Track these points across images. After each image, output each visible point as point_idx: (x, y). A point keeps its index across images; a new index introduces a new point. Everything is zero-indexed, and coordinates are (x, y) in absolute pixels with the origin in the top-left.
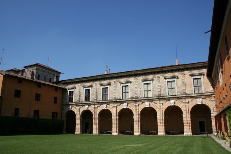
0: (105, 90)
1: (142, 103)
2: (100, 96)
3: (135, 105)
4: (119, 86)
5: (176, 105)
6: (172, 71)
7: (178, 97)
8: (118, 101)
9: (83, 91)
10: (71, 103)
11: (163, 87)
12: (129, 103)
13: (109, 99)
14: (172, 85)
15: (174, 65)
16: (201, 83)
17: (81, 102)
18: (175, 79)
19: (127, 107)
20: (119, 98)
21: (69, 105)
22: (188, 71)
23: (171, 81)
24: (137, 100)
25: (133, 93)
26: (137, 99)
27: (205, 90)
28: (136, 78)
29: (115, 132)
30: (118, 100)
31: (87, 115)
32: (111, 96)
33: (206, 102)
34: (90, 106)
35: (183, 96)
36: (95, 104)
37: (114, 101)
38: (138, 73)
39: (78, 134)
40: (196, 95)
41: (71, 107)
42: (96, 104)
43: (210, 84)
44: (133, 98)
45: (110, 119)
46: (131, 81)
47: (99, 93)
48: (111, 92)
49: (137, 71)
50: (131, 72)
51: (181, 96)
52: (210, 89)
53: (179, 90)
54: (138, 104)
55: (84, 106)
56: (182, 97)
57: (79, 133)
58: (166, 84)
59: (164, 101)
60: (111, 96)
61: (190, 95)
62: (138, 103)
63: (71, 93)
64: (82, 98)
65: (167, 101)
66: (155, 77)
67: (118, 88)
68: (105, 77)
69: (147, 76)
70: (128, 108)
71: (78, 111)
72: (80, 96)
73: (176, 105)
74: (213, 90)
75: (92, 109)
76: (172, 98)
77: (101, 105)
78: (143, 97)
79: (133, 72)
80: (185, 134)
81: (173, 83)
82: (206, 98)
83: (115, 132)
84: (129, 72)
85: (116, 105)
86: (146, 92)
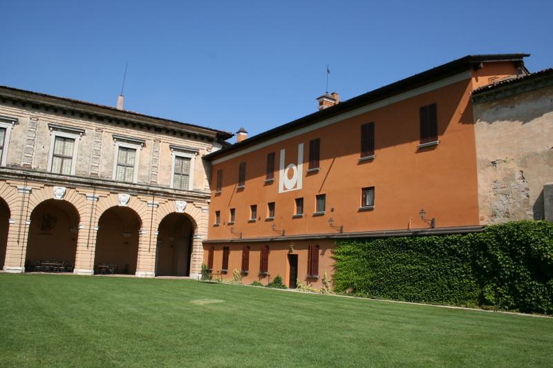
3: (22, 187)
5: (130, 206)
6: (134, 125)
7: (138, 189)
14: (126, 158)
15: (113, 107)
16: (188, 168)
18: (138, 147)
22: (169, 135)
23: (65, 139)
24: (29, 176)
25: (19, 153)
26: (31, 174)
27: (195, 185)
28: (36, 114)
33: (191, 210)
35: (151, 188)
38: (46, 102)
40: (177, 192)
43: (205, 176)
44: (15, 166)
45: (161, 242)
46: (17, 119)
49: (46, 98)
51: (145, 188)
53: (143, 174)
58: (114, 152)
59: (105, 193)
61: (165, 190)
62: (30, 186)
66: (91, 127)
74: (208, 188)
76: (124, 188)
78: (49, 171)
79: (31, 96)
80: (140, 274)
81: (130, 154)
82: (77, 189)
84: (20, 93)
86: (58, 161)
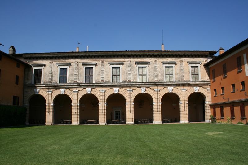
0: (89, 71)
1: (109, 88)
2: (82, 78)
3: (129, 90)
4: (108, 68)
5: (174, 92)
6: (170, 56)
7: (176, 84)
8: (106, 85)
9: (58, 70)
10: (39, 85)
11: (160, 73)
12: (121, 88)
13: (94, 82)
14: (169, 71)
15: (160, 50)
16: (198, 71)
17: (55, 84)
18: (173, 66)
19: (118, 92)
20: (107, 81)
21: (36, 87)
22: (186, 58)
23: (142, 67)
24: (131, 85)
25: (126, 76)
26: (131, 84)
27: (202, 78)
28: (130, 59)
29: (103, 122)
30: (108, 84)
31: (63, 103)
32: (96, 78)
33: (202, 91)
34: (67, 90)
35: (182, 83)
36: (75, 88)
37: (101, 84)
38: (133, 54)
39: (50, 125)
40: (194, 83)
41: (38, 90)
42: (76, 88)
43: (206, 74)
44: (125, 82)
45: (190, 106)
47: (80, 74)
48: (97, 73)
49: (132, 52)
50: (125, 52)
51: (179, 83)
52: (206, 78)
53: (177, 77)
54: (131, 90)
55: (59, 89)
56: (180, 84)
57: (51, 124)
58: (163, 69)
59: (162, 88)
60: (96, 78)
61: (189, 83)
62: (132, 89)
63: (39, 72)
64: (56, 79)
65: (165, 87)
66: (152, 60)
67: (106, 70)
68: (90, 54)
69: (143, 59)
70: (120, 93)
71: (49, 96)
72: (52, 76)
73: (174, 92)
74: (209, 79)
75: (70, 93)
76: (170, 84)
77: (84, 88)
78: (138, 82)
79: (127, 52)
80: (182, 122)
81: (170, 69)
82: (150, 88)
83: (130, 121)
84: (122, 52)
85: (104, 89)
86: (141, 77)
